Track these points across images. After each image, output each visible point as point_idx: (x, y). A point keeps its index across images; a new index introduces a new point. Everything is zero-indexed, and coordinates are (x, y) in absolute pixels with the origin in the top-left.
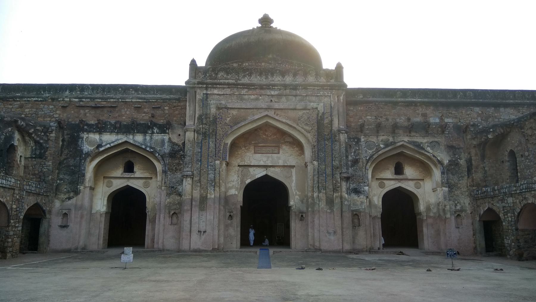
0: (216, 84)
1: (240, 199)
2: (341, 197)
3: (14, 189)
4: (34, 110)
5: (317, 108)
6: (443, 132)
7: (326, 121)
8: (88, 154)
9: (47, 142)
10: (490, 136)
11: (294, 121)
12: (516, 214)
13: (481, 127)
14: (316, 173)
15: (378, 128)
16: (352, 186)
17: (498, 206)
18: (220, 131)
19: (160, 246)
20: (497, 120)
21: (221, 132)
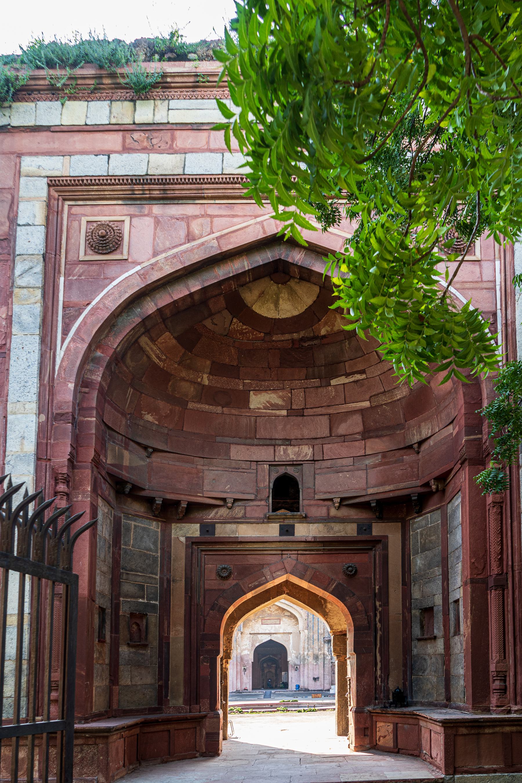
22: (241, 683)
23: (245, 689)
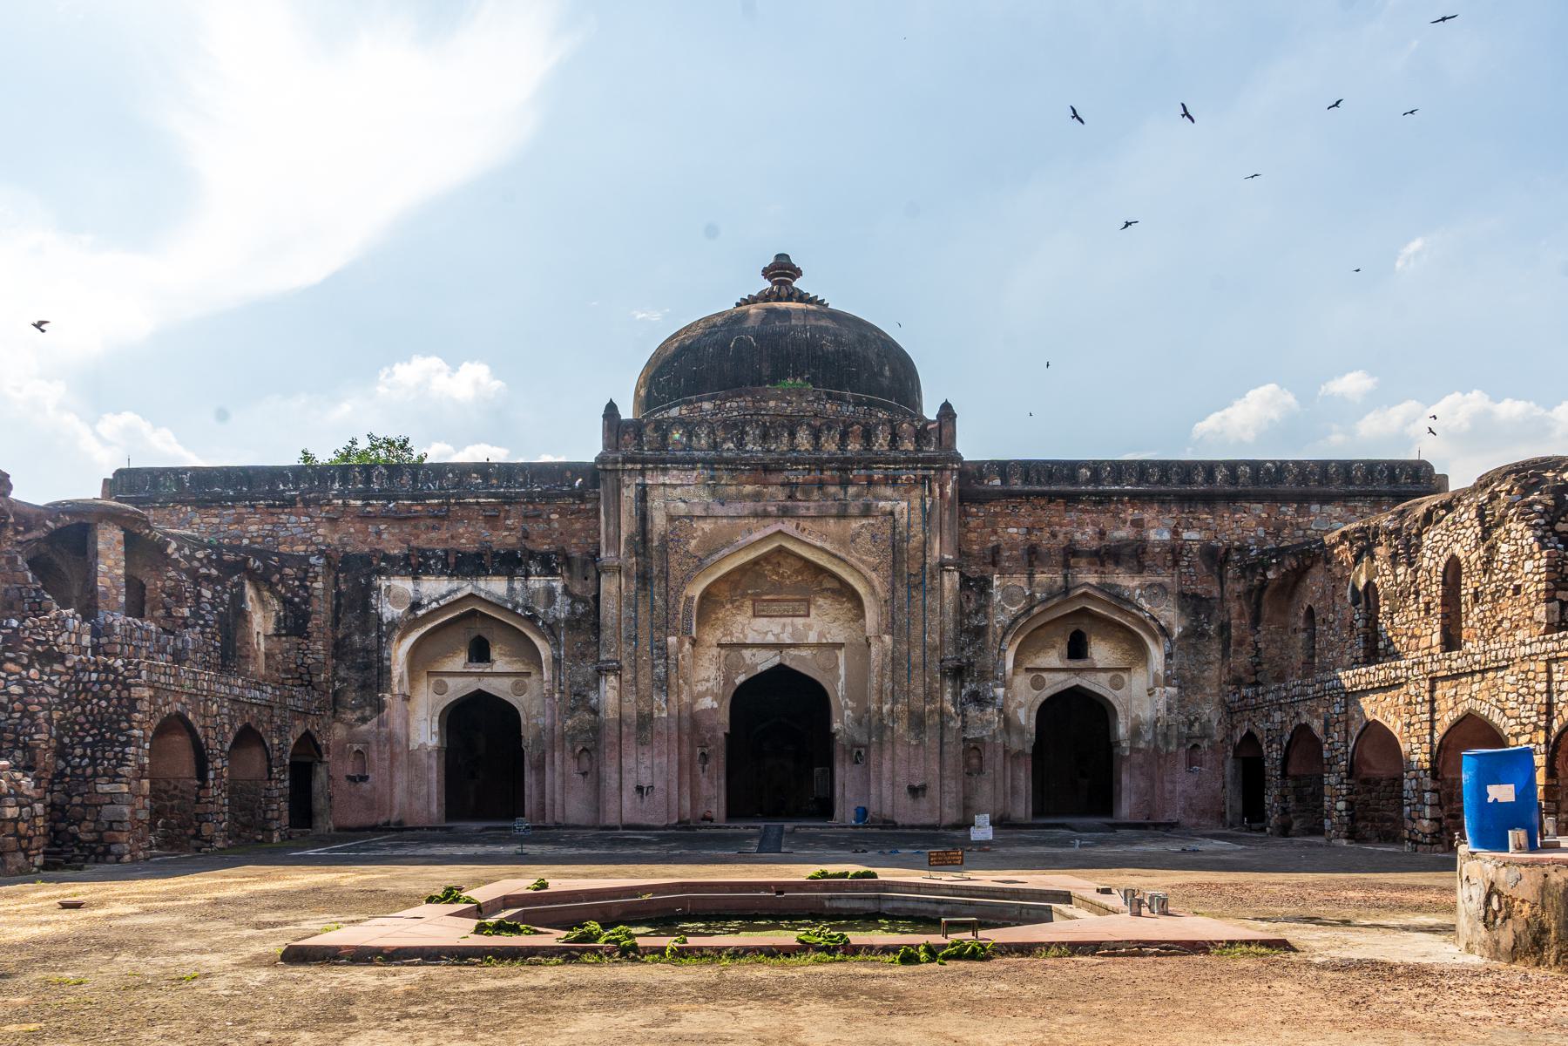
0: (664, 461)
1: (724, 718)
2: (942, 712)
3: (271, 708)
4: (269, 527)
5: (892, 513)
6: (1176, 563)
7: (914, 543)
8: (393, 625)
9: (306, 601)
10: (1271, 575)
11: (842, 543)
14: (888, 659)
15: (1033, 557)
16: (970, 686)
18: (675, 570)
19: (558, 819)
21: (678, 574)
22: (694, 800)
23: (705, 818)
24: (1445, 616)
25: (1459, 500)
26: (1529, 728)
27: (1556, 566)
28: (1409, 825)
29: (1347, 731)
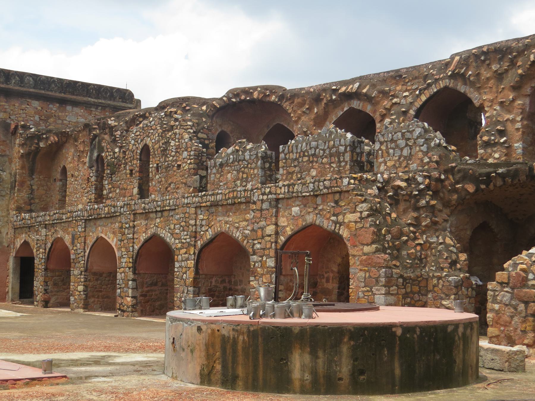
10: (42, 145)
12: (47, 250)
13: (33, 130)
17: (33, 238)
20: (60, 122)
24: (141, 179)
25: (150, 114)
26: (186, 245)
27: (198, 156)
28: (119, 300)
29: (85, 243)
